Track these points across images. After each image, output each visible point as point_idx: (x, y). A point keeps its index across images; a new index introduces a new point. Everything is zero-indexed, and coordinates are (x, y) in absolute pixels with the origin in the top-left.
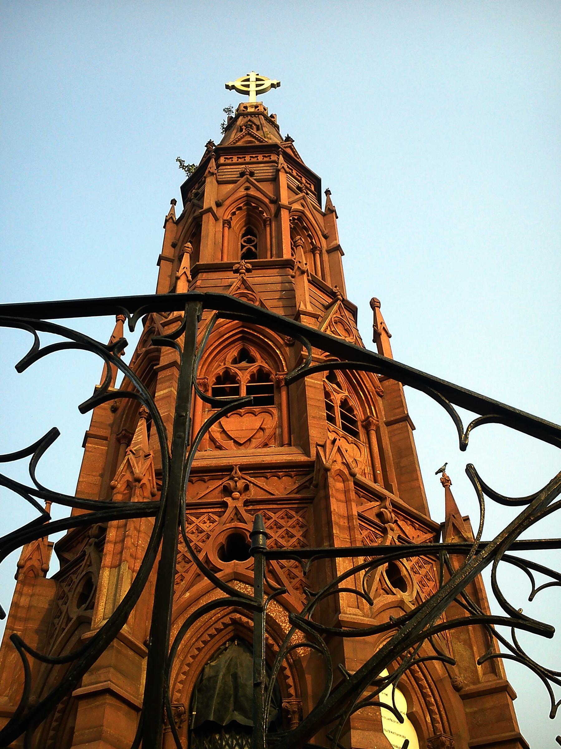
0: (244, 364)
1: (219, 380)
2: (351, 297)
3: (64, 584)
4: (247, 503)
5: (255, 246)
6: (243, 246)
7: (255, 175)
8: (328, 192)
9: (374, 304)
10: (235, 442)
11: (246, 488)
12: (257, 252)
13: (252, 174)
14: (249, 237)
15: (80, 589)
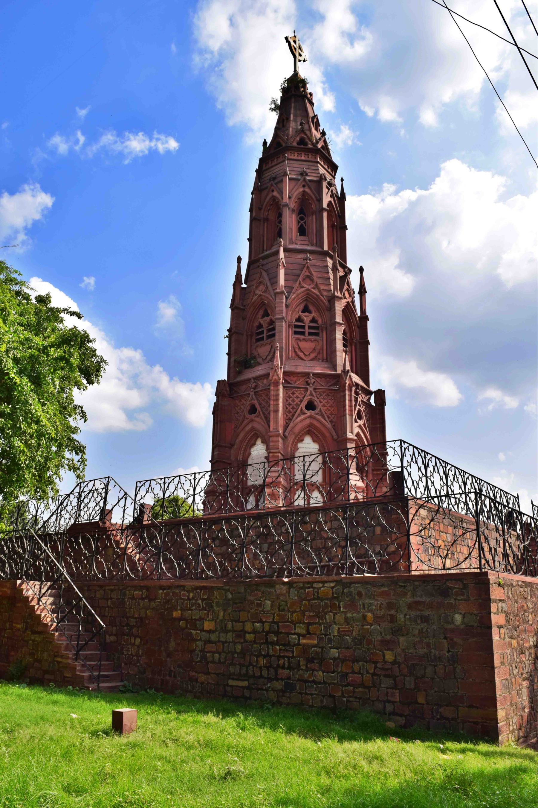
0: (307, 314)
1: (297, 320)
2: (349, 264)
3: (237, 401)
4: (315, 389)
5: (305, 223)
6: (299, 222)
7: (309, 174)
8: (342, 180)
9: (361, 270)
10: (304, 354)
11: (314, 382)
12: (306, 227)
13: (307, 175)
14: (302, 215)
15: (249, 408)
